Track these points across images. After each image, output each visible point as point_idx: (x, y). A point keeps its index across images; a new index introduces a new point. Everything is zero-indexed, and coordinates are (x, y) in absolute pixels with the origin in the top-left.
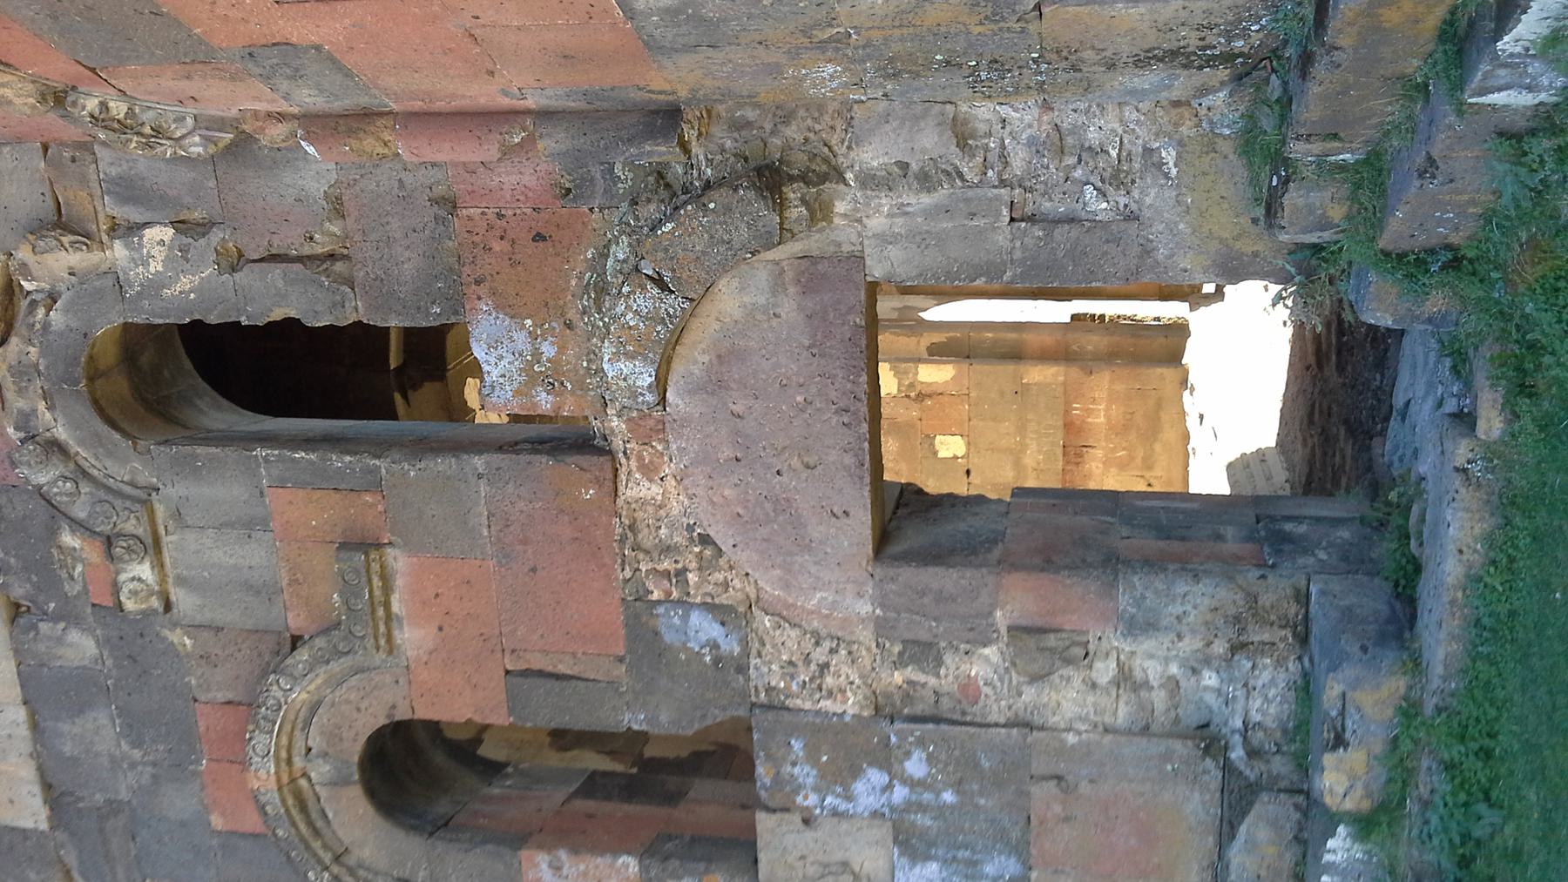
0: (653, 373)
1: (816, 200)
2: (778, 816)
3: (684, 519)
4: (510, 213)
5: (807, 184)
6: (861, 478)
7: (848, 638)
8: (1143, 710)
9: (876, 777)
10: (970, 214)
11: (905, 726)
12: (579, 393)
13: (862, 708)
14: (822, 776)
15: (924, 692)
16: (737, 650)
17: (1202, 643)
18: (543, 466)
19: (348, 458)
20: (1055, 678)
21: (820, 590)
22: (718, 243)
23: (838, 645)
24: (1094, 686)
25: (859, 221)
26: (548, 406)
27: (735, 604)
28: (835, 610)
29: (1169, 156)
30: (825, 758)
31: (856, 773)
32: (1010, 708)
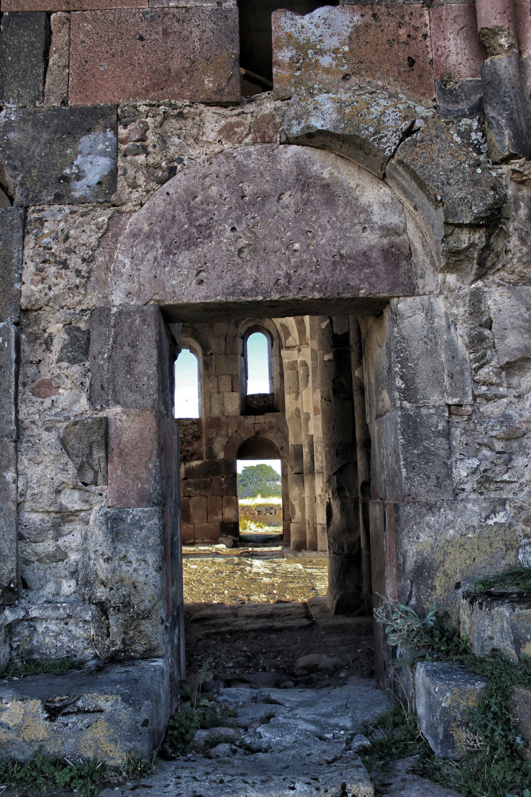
0: (324, 128)
1: (467, 256)
3: (186, 158)
5: (483, 250)
6: (232, 294)
7: (89, 285)
8: (38, 534)
10: (452, 374)
11: (13, 334)
12: (293, 81)
13: (28, 297)
15: (40, 351)
17: (104, 578)
18: (230, 50)
20: (65, 458)
21: (132, 263)
22: (447, 175)
23: (83, 277)
24: (58, 492)
25: (441, 293)
26: (280, 58)
27: (118, 192)
28: (114, 274)
29: (500, 518)
32: (33, 422)
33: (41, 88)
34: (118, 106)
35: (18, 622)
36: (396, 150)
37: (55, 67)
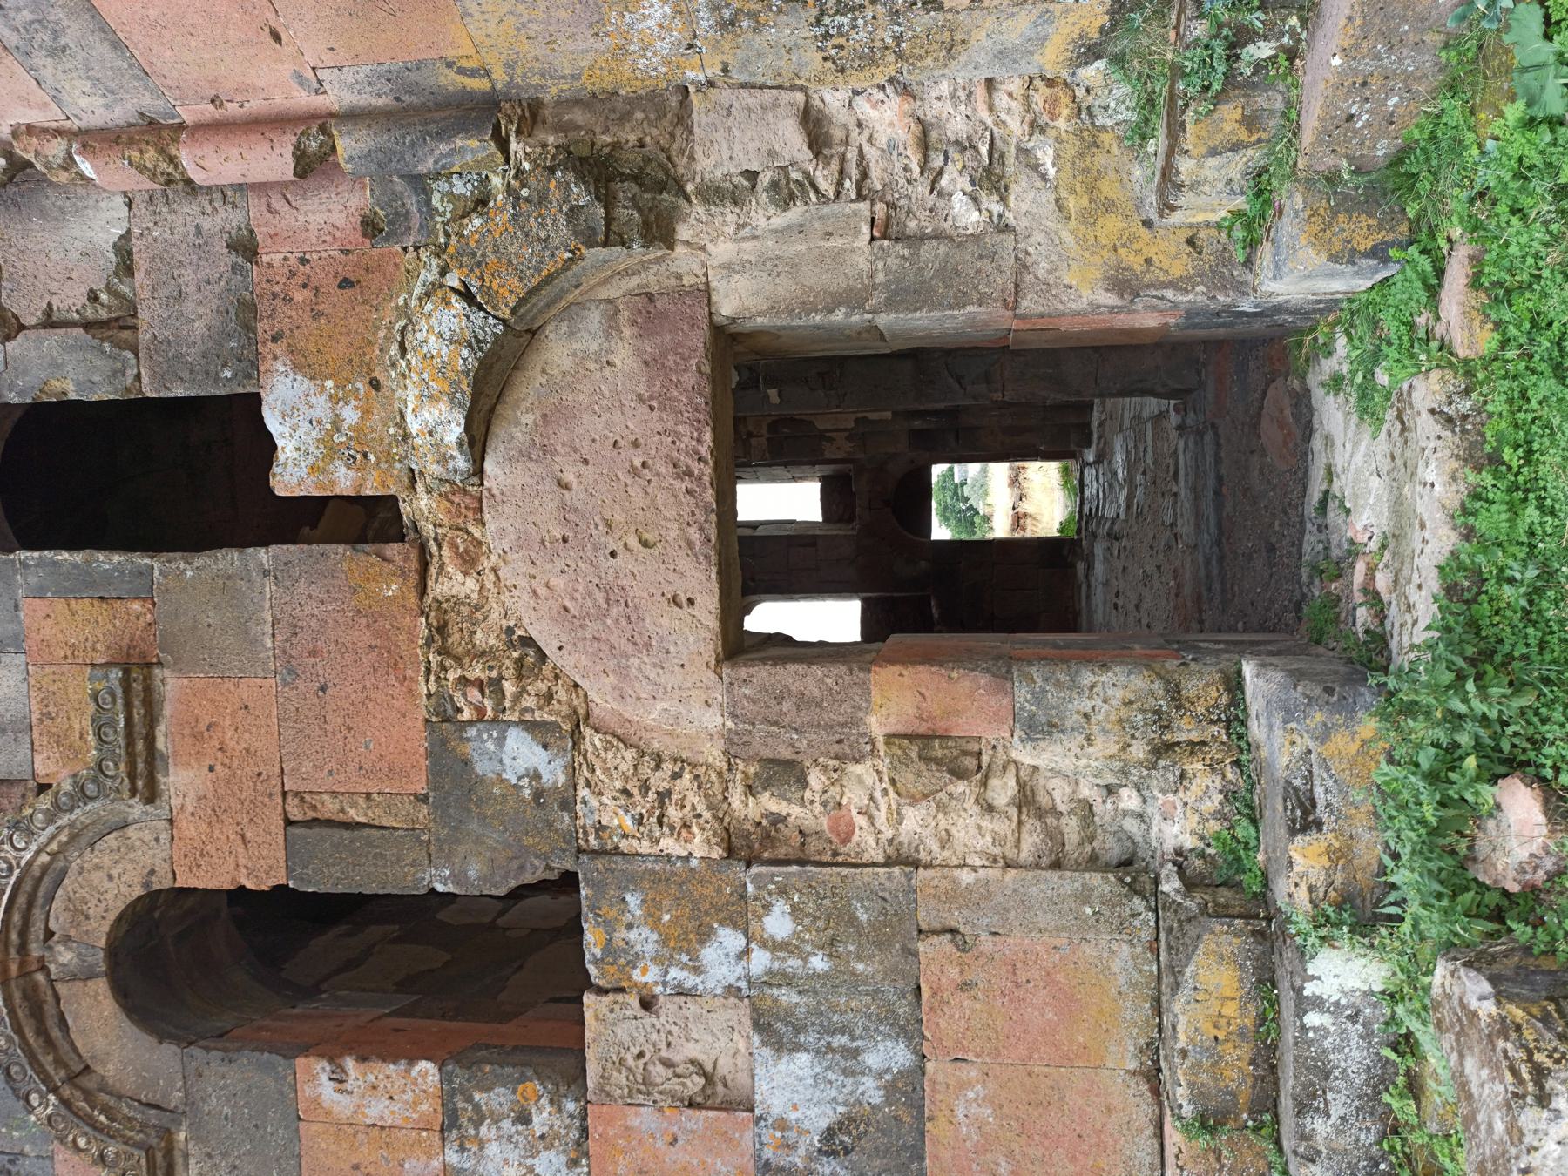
2: (611, 997)
4: (315, 256)
5: (640, 185)
9: (731, 939)
11: (763, 869)
14: (664, 942)
16: (562, 779)
19: (117, 558)
23: (682, 769)
24: (990, 809)
25: (703, 249)
29: (1046, 157)
30: (667, 917)
31: (705, 935)
33: (401, 833)
34: (427, 721)
35: (1181, 870)
36: (495, 317)
37: (370, 813)
